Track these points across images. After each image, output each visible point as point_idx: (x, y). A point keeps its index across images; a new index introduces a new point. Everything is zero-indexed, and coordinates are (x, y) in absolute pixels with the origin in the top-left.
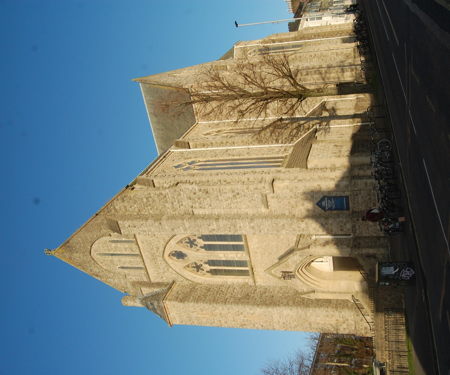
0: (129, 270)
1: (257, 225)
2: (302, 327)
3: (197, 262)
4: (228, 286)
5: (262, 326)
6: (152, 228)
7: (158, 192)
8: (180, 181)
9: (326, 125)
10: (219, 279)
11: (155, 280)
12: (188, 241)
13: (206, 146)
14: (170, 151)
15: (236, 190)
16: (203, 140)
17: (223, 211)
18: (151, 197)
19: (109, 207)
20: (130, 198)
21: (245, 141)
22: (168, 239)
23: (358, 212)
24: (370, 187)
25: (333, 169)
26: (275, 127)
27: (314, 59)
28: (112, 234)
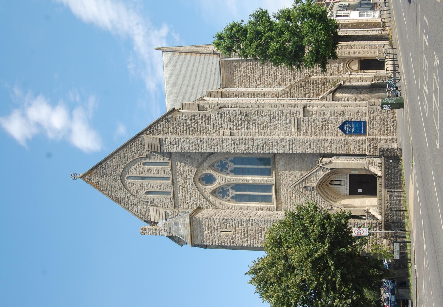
12: (220, 164)
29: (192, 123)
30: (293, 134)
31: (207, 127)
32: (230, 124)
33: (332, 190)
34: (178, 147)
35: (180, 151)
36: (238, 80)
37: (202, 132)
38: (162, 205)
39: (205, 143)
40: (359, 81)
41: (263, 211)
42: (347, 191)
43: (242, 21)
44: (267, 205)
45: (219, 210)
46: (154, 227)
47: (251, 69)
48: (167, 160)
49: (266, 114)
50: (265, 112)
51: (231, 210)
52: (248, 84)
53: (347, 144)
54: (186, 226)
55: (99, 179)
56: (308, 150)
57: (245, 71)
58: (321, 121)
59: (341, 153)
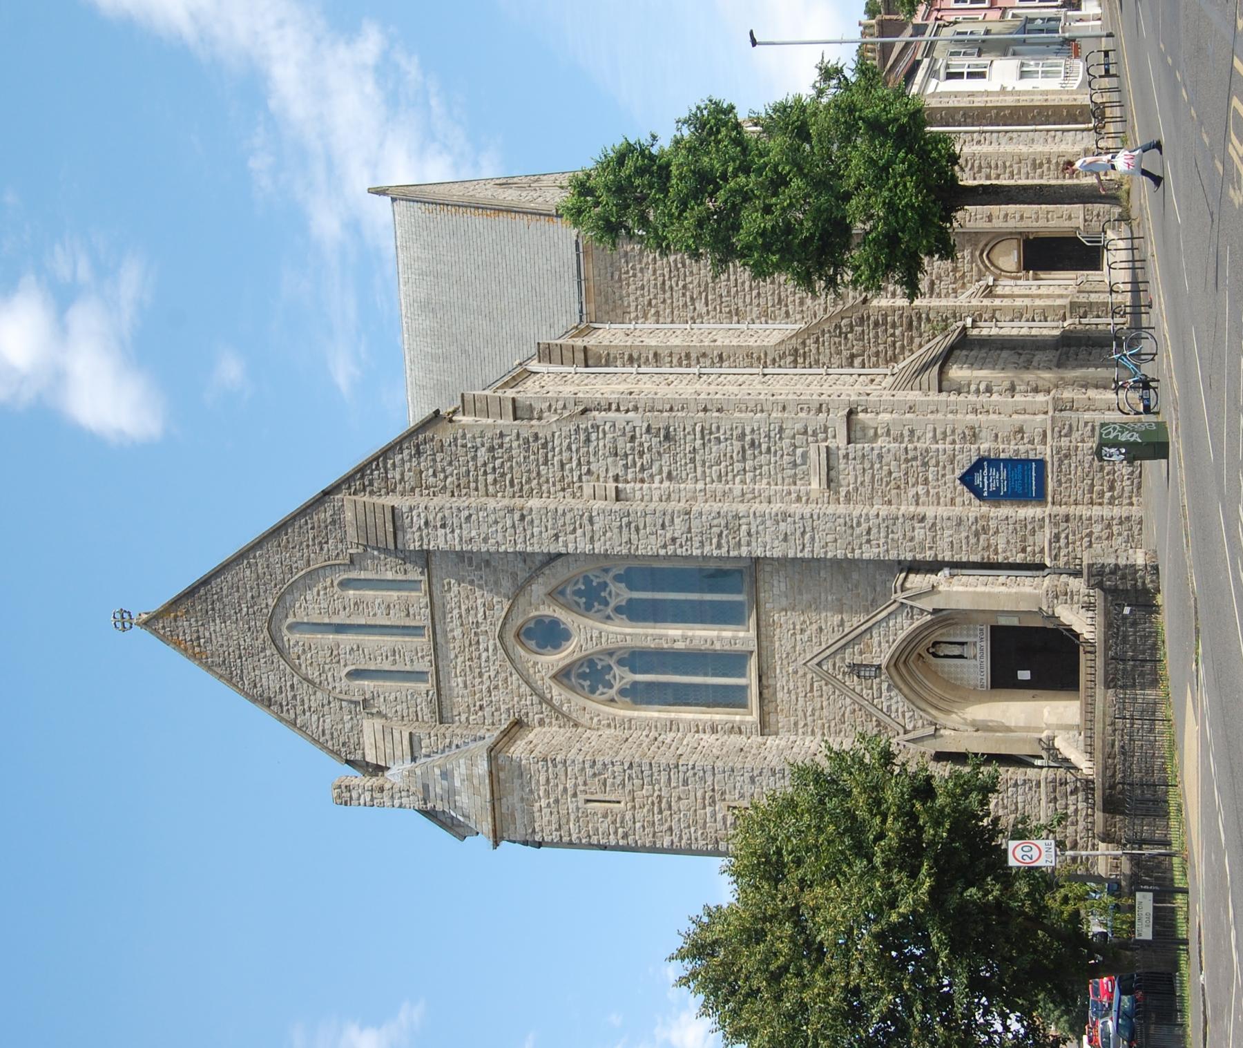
12: (583, 587)
29: (494, 458)
30: (813, 496)
31: (543, 473)
32: (615, 464)
33: (936, 673)
34: (449, 536)
35: (458, 548)
36: (637, 299)
37: (526, 487)
38: (399, 713)
39: (535, 524)
40: (1024, 319)
41: (718, 736)
42: (984, 677)
43: (654, 138)
44: (731, 718)
45: (580, 729)
46: (374, 779)
47: (676, 265)
48: (415, 574)
49: (729, 433)
50: (725, 426)
51: (618, 732)
52: (668, 311)
53: (985, 530)
54: (476, 781)
55: (201, 629)
56: (860, 548)
57: (658, 272)
58: (903, 458)
59: (964, 559)
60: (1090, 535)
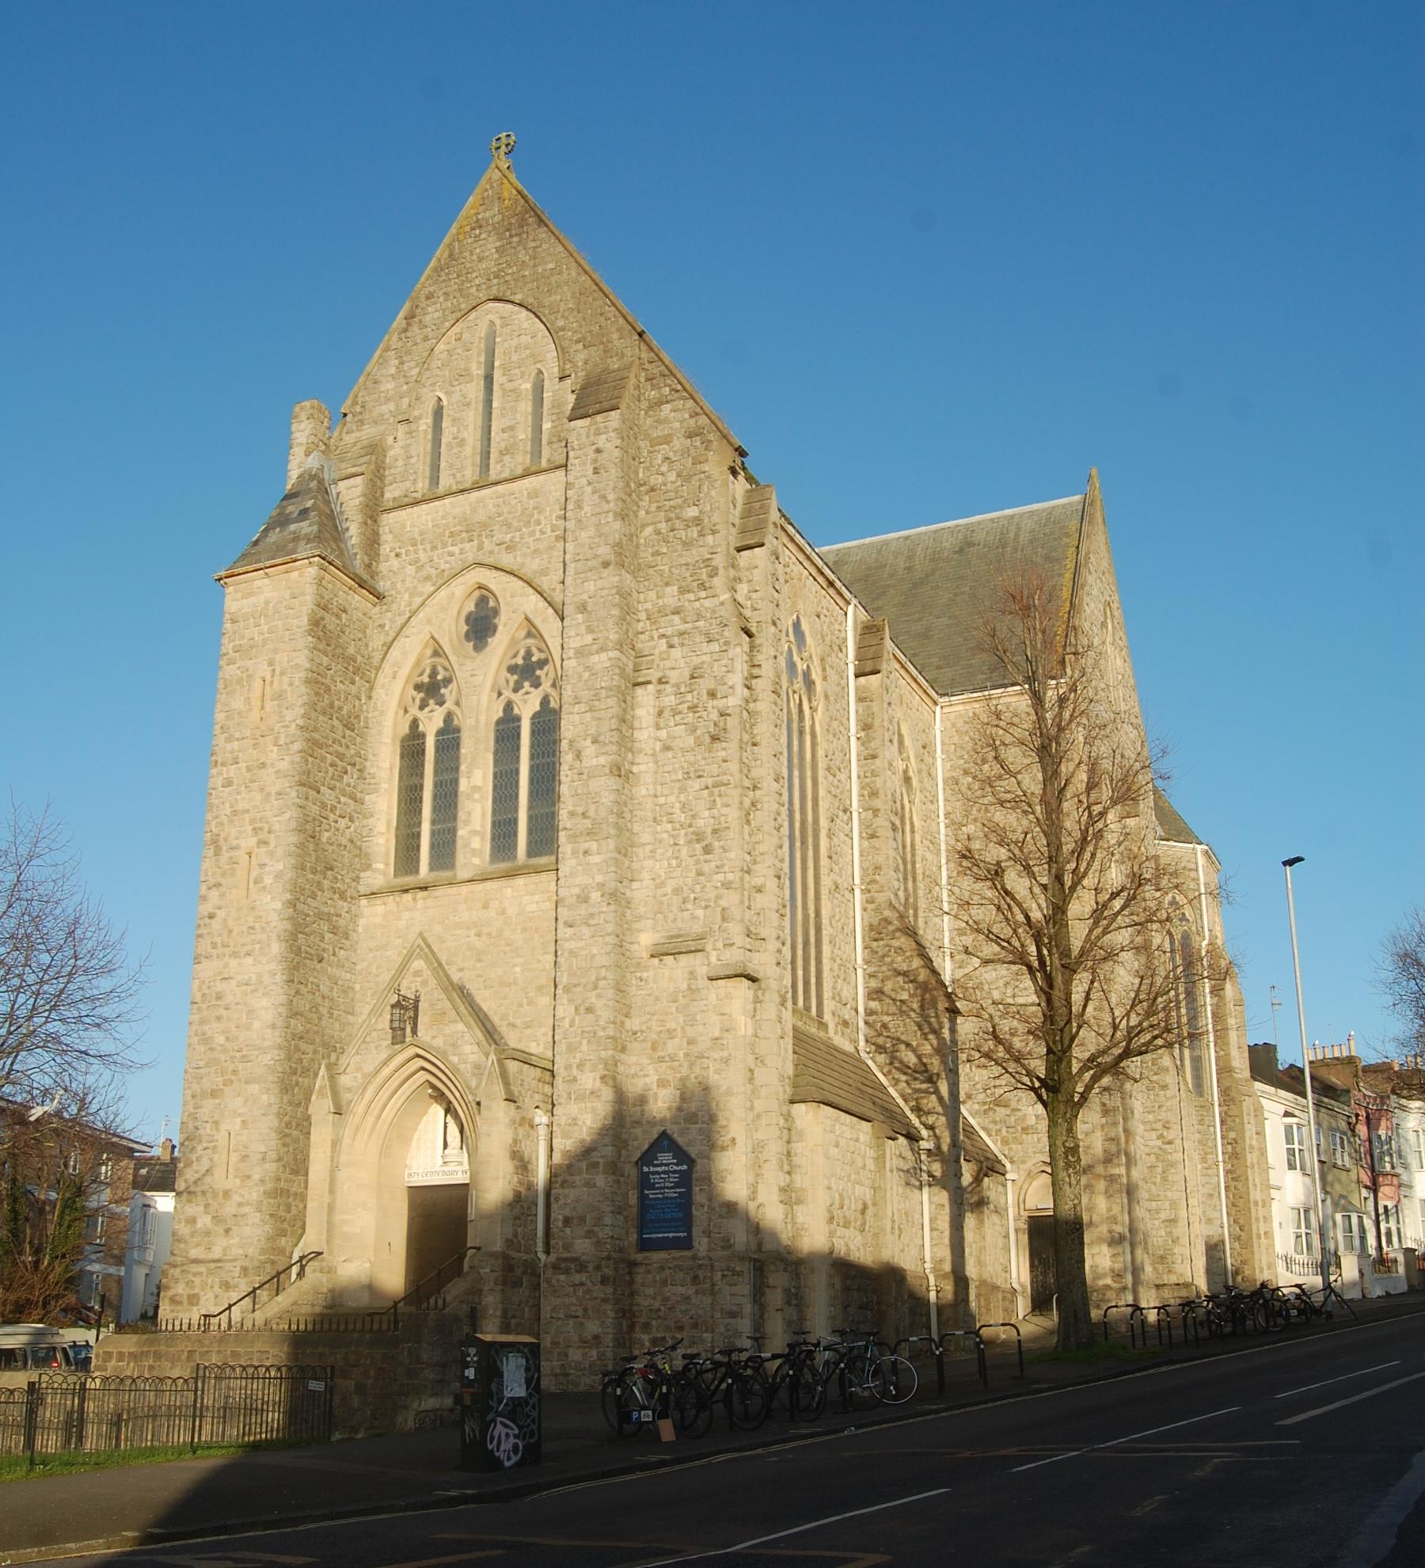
0: (430, 437)
1: (592, 915)
2: (202, 1064)
3: (453, 686)
4: (359, 795)
5: (211, 916)
6: (592, 534)
7: (719, 560)
8: (758, 641)
9: (930, 1175)
10: (387, 765)
11: (387, 529)
12: (534, 659)
13: (862, 734)
14: (848, 603)
15: (721, 843)
16: (886, 724)
17: (644, 792)
18: (702, 535)
19: (668, 382)
20: (702, 459)
21: (877, 877)
22: (545, 587)
23: (631, 1282)
24: (722, 1329)
25: (790, 1196)
26: (924, 987)
27: (1154, 1135)
28: (568, 382)
42: (420, 1178)
60: (586, 1315)
